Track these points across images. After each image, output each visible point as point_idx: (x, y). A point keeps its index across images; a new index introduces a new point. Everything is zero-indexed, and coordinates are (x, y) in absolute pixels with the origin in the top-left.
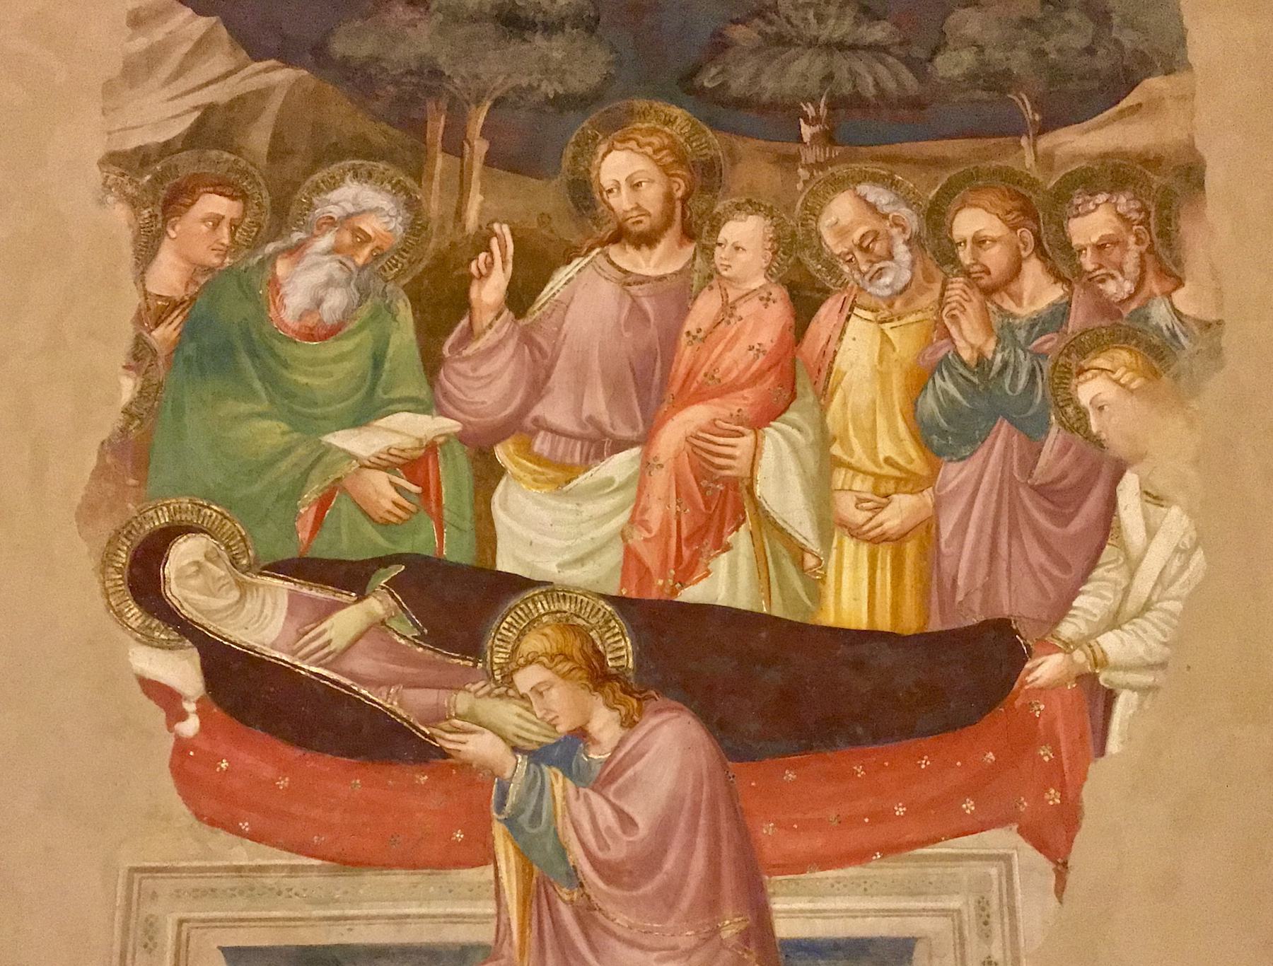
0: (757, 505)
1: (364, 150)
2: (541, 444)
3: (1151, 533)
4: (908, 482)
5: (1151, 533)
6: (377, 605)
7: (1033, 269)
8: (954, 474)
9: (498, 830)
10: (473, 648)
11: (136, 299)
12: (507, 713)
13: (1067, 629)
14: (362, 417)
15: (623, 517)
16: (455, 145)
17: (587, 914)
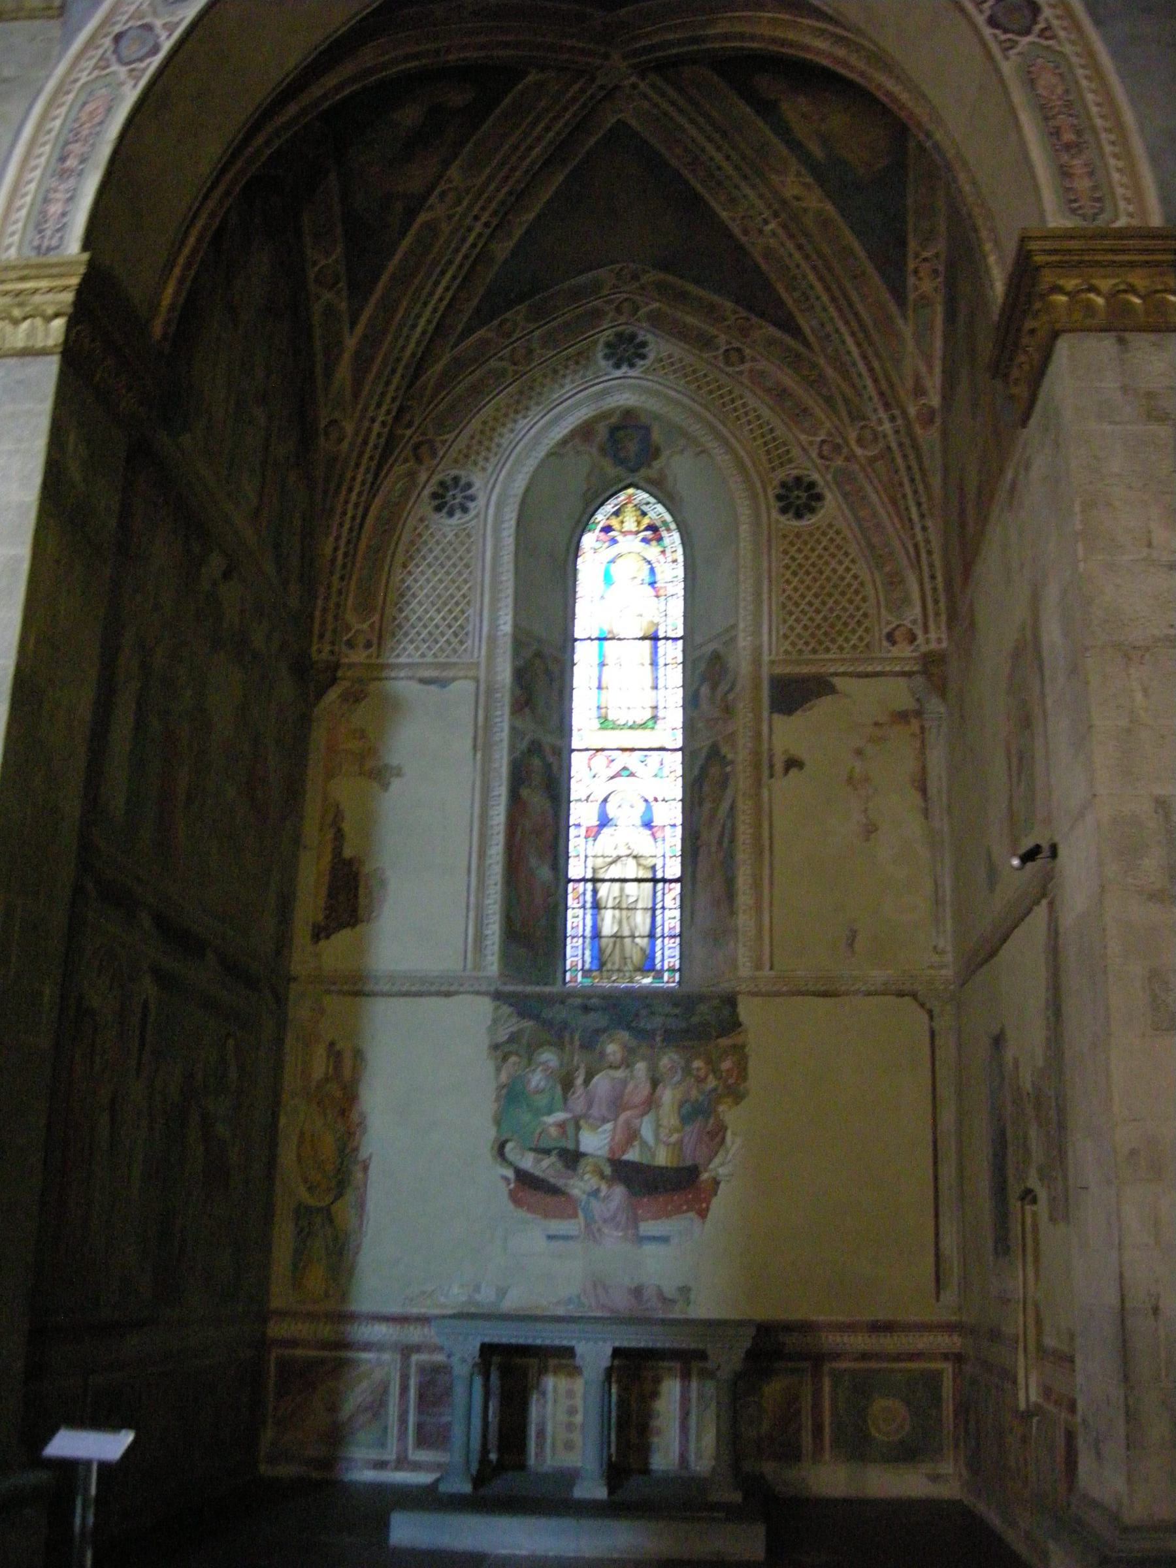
0: (641, 1137)
1: (550, 1044)
2: (591, 1121)
3: (733, 1144)
4: (677, 1131)
5: (733, 1144)
6: (553, 1158)
7: (711, 1076)
8: (688, 1128)
9: (580, 1212)
10: (574, 1169)
11: (494, 1085)
12: (581, 1184)
13: (711, 1166)
14: (550, 1112)
15: (609, 1139)
16: (572, 1042)
17: (599, 1230)
